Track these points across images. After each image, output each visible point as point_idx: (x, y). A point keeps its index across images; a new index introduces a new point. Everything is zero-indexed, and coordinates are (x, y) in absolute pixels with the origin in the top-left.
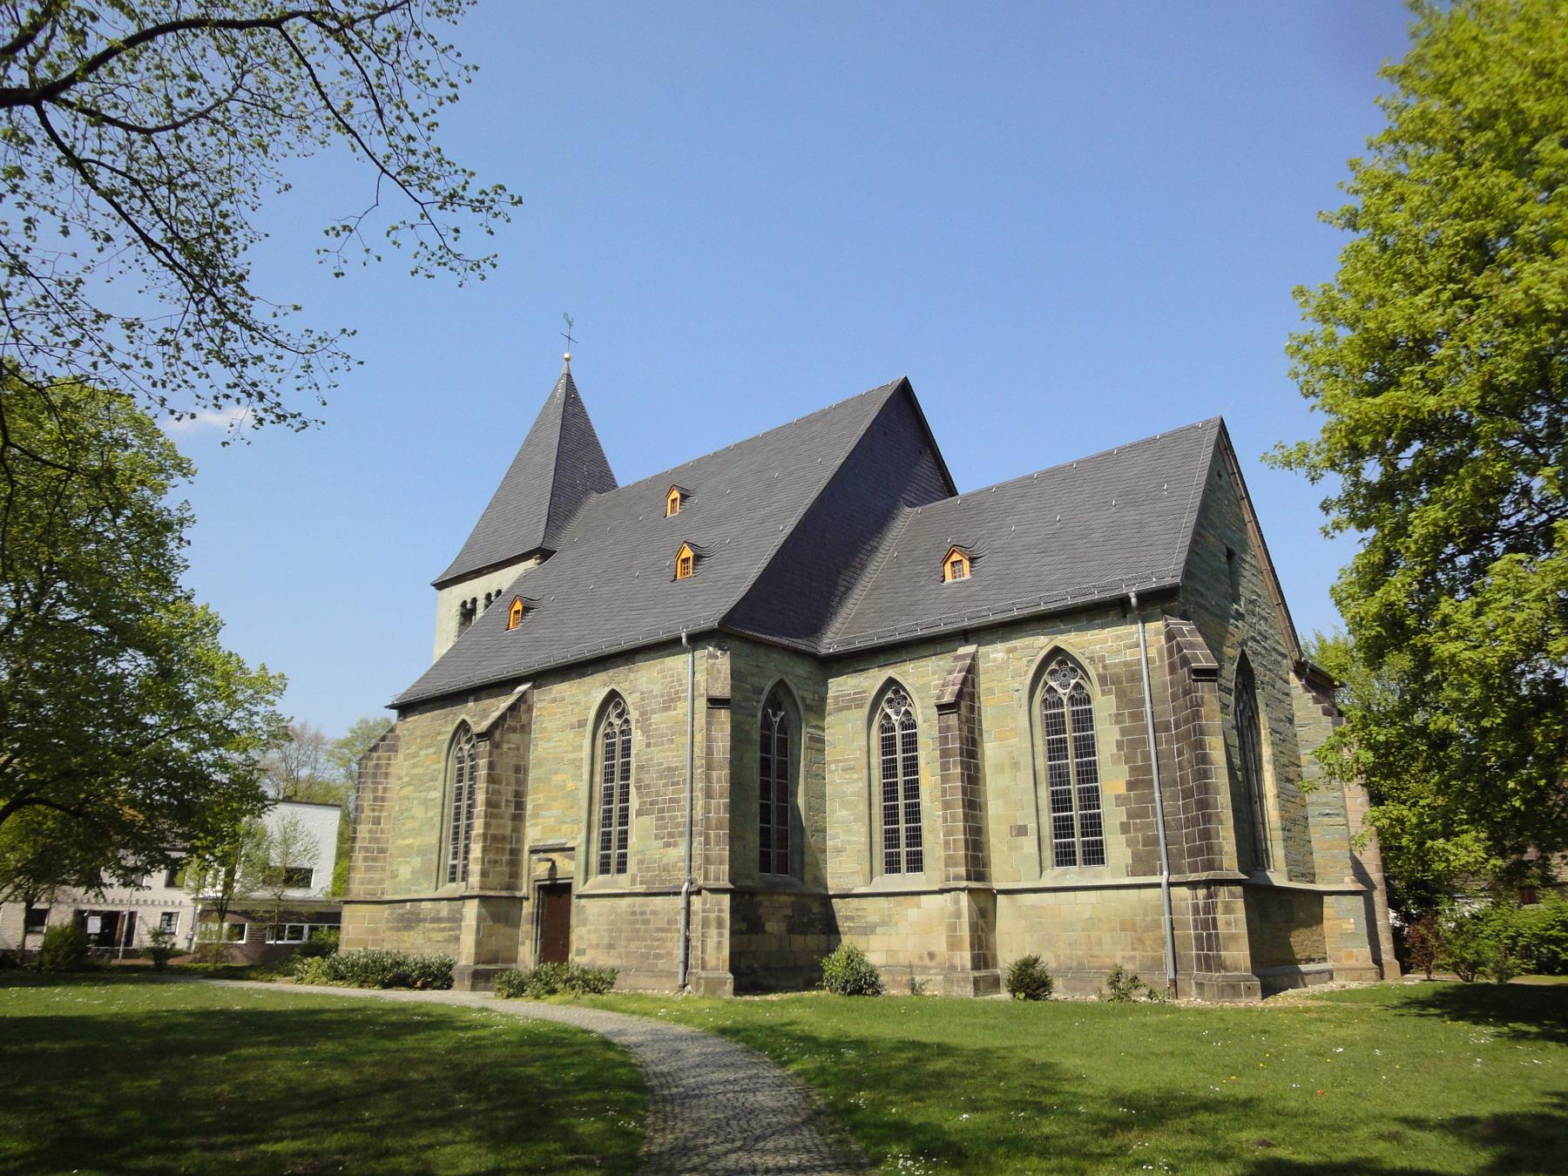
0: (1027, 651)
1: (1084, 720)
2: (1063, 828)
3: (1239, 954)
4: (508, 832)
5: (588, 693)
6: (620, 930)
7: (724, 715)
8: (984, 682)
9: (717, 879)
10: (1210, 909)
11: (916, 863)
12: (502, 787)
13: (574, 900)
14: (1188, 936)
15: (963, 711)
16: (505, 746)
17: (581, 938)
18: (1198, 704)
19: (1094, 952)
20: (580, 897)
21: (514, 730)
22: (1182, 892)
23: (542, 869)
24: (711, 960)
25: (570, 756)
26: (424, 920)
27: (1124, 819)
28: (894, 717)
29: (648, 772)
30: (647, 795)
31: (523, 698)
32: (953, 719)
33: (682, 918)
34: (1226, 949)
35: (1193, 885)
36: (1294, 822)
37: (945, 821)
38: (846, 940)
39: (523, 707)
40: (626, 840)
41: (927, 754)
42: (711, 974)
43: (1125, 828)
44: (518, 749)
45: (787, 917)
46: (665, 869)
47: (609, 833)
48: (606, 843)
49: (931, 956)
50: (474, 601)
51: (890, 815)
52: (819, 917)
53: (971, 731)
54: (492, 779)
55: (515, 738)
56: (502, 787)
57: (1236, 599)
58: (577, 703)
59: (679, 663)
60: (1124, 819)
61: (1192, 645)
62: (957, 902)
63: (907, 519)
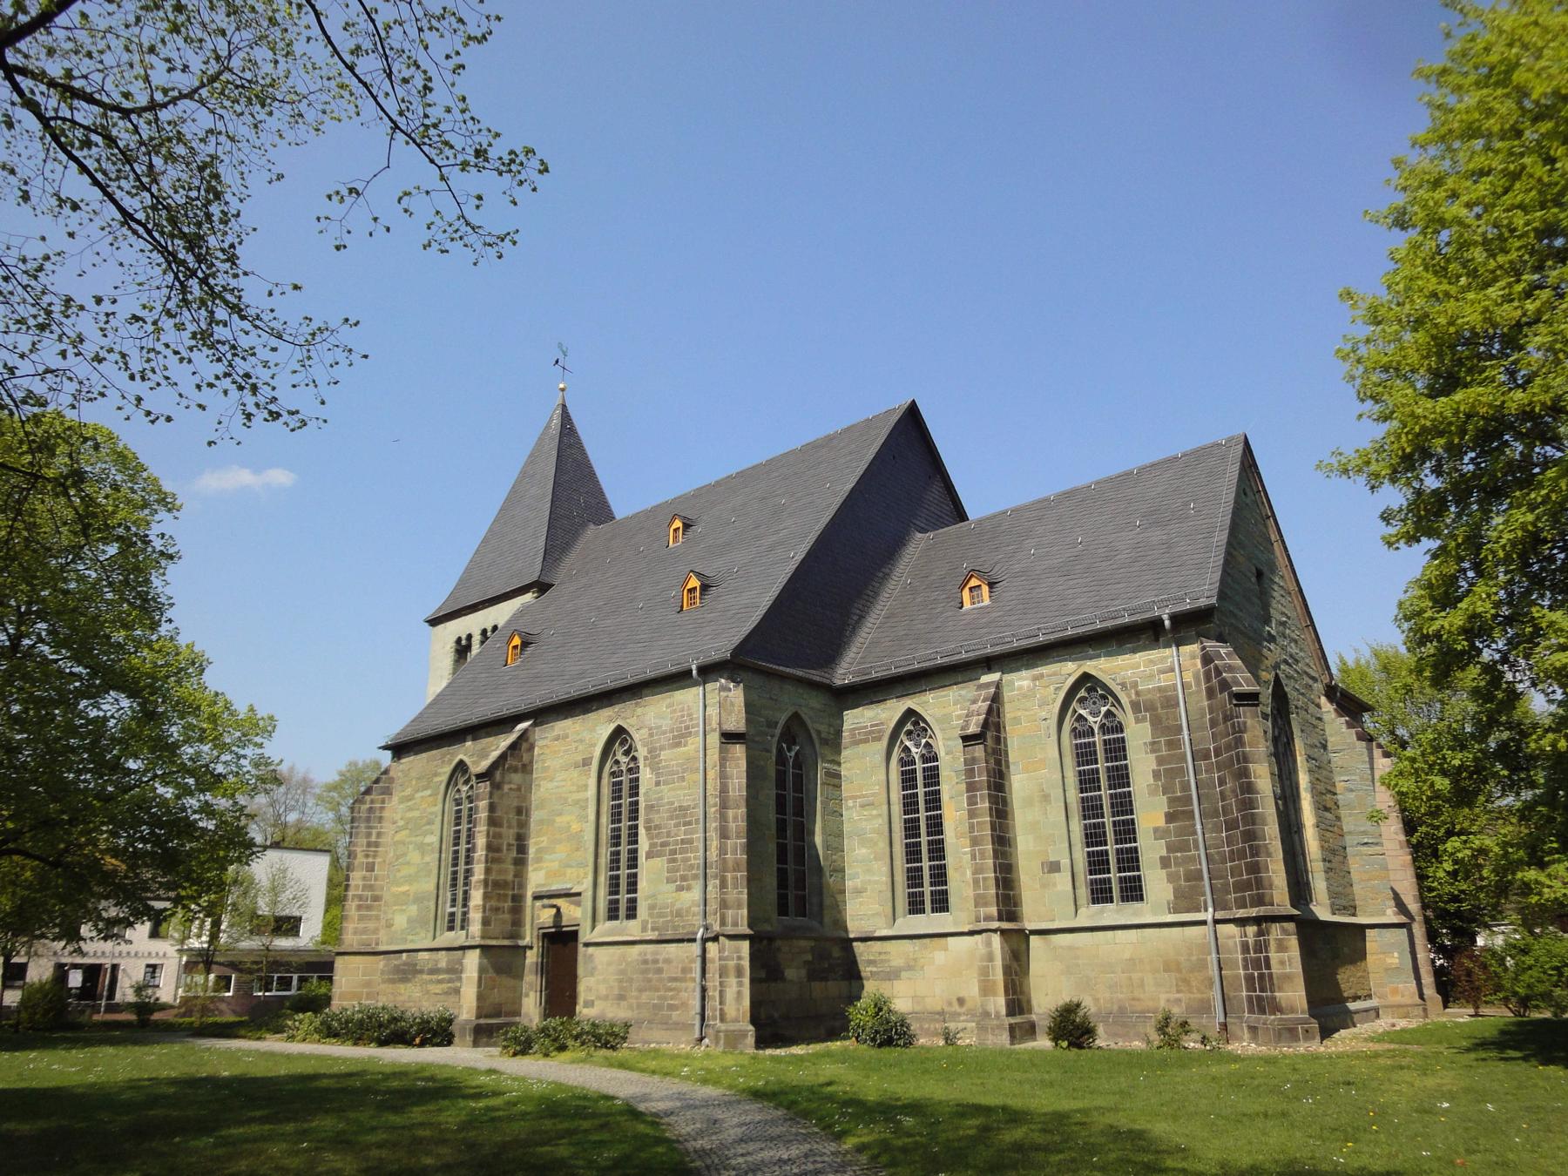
0: (1054, 678)
1: (1117, 750)
2: (1097, 863)
3: (1294, 995)
4: (510, 877)
5: (593, 730)
6: (631, 980)
7: (739, 751)
8: (1009, 712)
9: (735, 924)
10: (1261, 947)
11: (941, 903)
12: (504, 830)
13: (581, 949)
14: (1237, 977)
15: (990, 742)
16: (506, 787)
17: (589, 989)
18: (1240, 730)
19: (1136, 994)
20: (587, 945)
21: (516, 770)
22: (1231, 929)
23: (546, 916)
24: (731, 1011)
25: (576, 796)
26: (421, 972)
27: (1164, 853)
28: (914, 750)
29: (658, 812)
30: (658, 836)
31: (524, 735)
32: (979, 751)
33: (697, 966)
34: (1280, 990)
35: (1242, 922)
36: (1333, 852)
37: (974, 857)
38: (870, 987)
39: (525, 746)
40: (635, 883)
41: (951, 789)
42: (732, 1027)
43: (1165, 862)
44: (519, 789)
45: (806, 962)
46: (679, 914)
47: (618, 877)
48: (614, 886)
49: (961, 1001)
50: (469, 637)
51: (913, 853)
52: (839, 963)
53: (998, 762)
54: (492, 822)
55: (517, 778)
56: (504, 830)
57: (1267, 620)
58: (581, 741)
59: (689, 697)
60: (1164, 853)
61: (1231, 669)
62: (989, 944)
63: (919, 542)
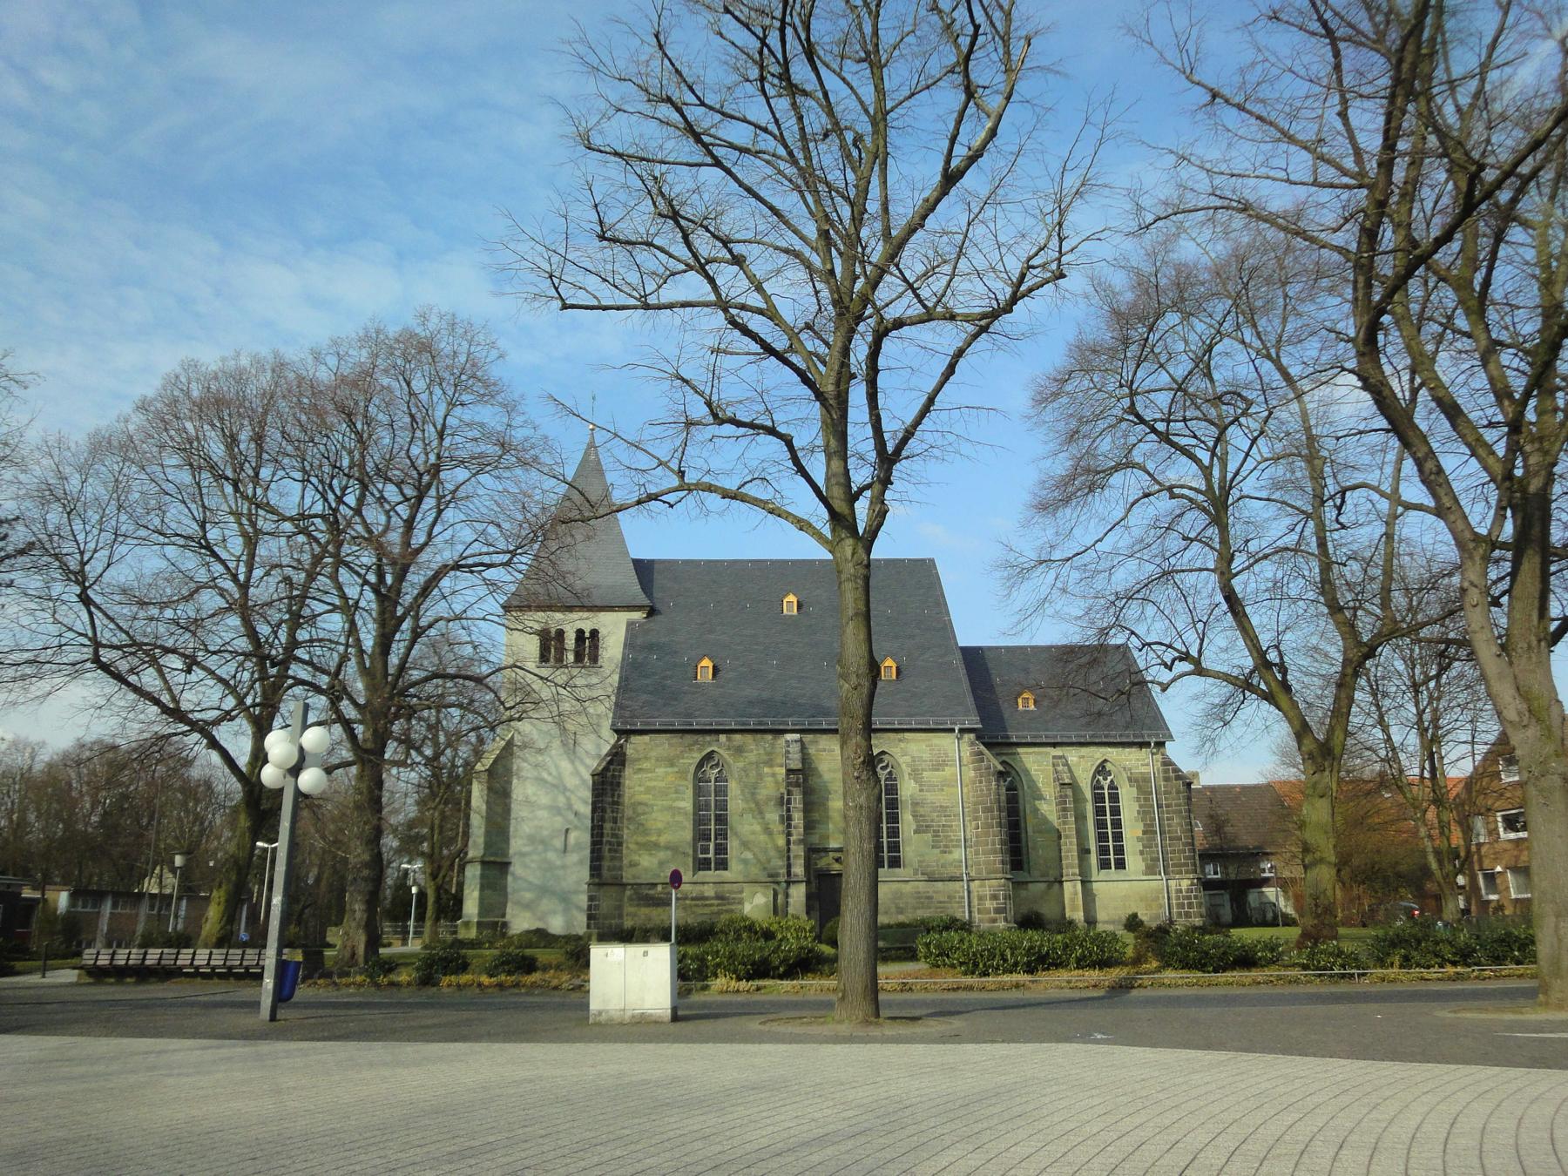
1: (1115, 798)
43: (1142, 853)
59: (947, 743)
